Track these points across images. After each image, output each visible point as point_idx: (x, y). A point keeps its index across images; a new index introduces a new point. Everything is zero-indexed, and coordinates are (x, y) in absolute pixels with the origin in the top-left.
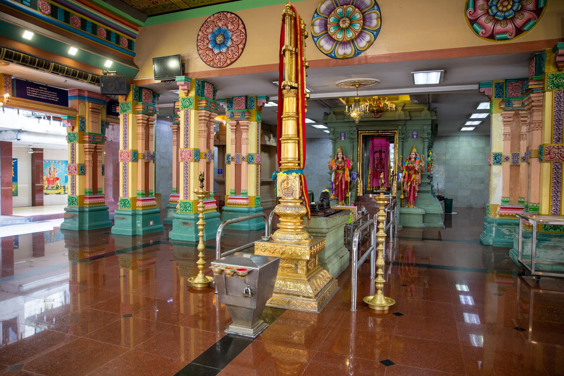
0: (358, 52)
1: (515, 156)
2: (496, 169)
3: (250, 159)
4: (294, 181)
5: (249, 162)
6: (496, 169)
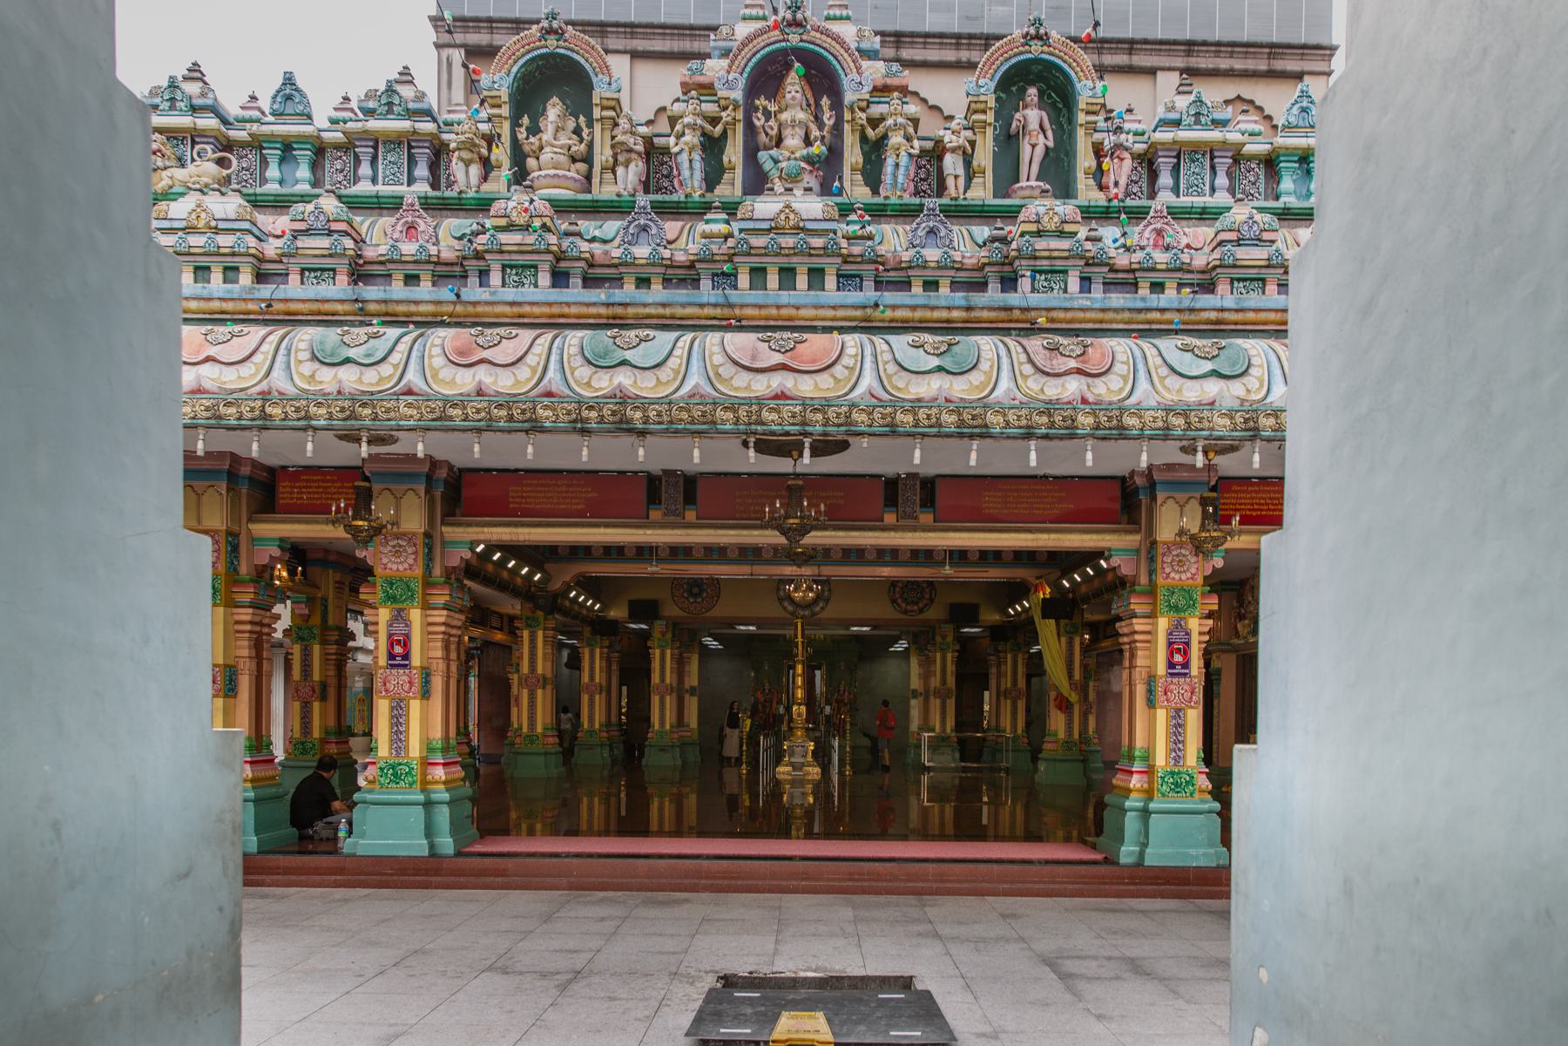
0: (814, 614)
1: (927, 692)
2: (913, 702)
3: (692, 691)
4: (803, 708)
5: (692, 695)
6: (913, 702)
